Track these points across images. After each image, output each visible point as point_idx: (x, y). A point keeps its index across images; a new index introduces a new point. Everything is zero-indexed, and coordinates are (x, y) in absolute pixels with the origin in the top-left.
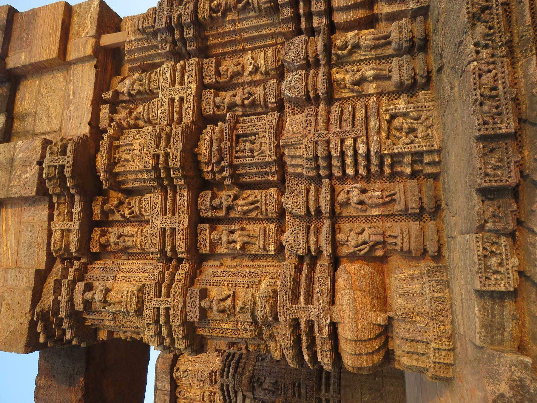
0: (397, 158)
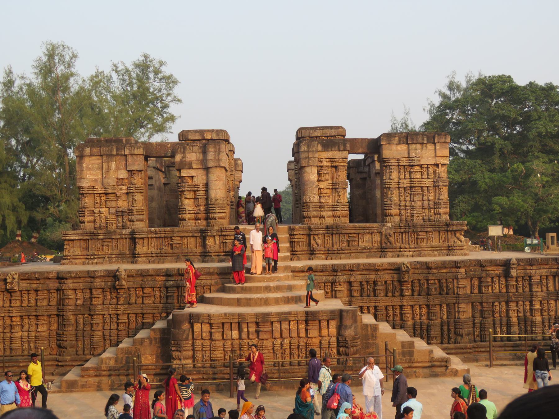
0: (413, 217)
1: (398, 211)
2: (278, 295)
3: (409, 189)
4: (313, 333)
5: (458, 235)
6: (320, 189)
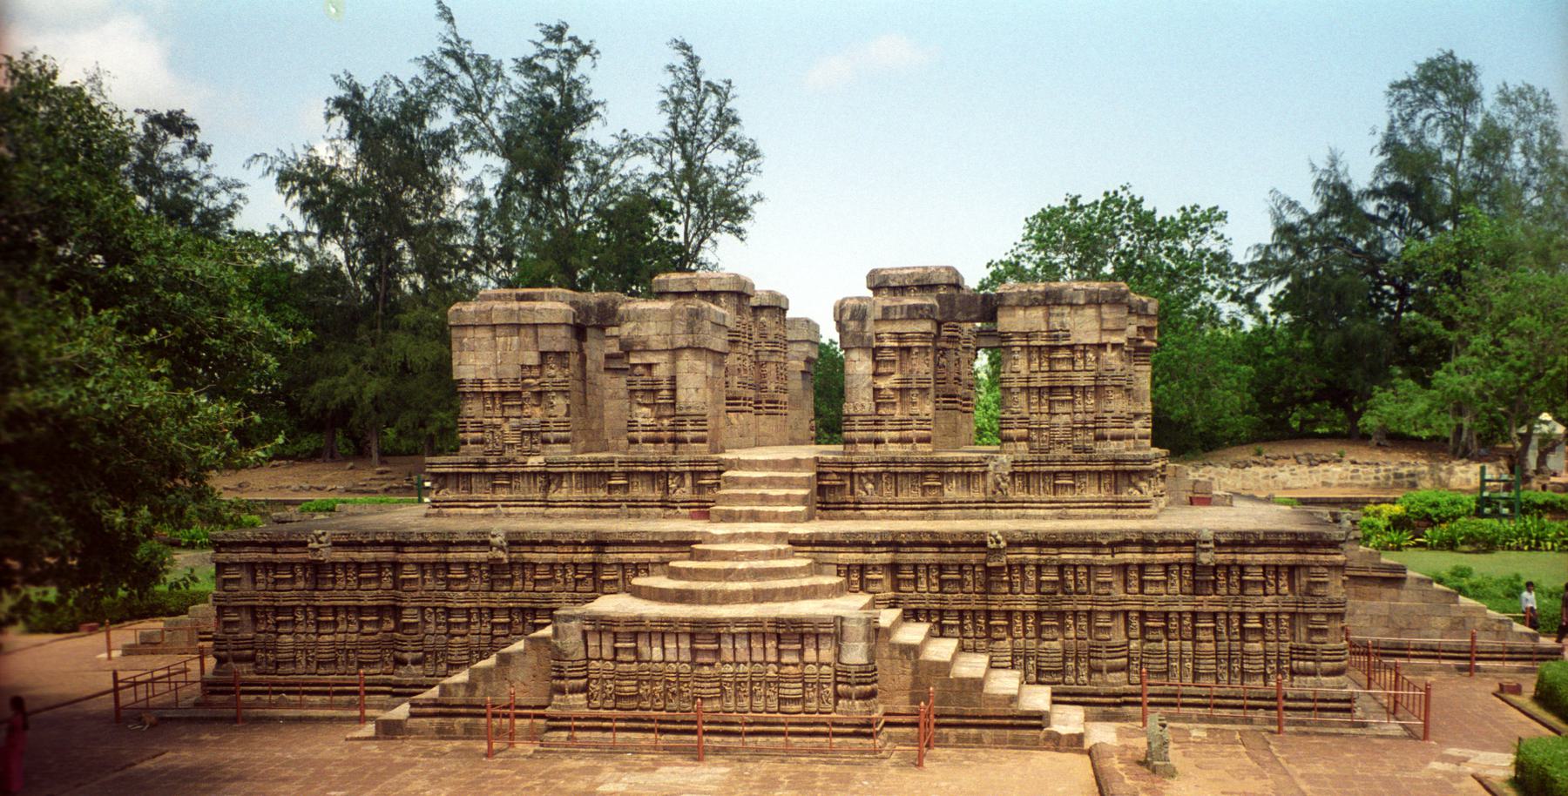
2: (745, 586)
5: (1134, 479)
6: (876, 391)
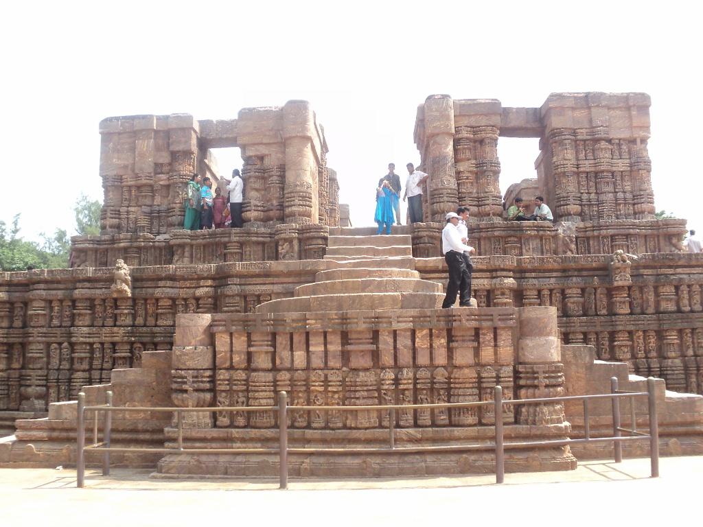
1: (579, 208)
3: (593, 175)
4: (464, 356)
5: (674, 241)
